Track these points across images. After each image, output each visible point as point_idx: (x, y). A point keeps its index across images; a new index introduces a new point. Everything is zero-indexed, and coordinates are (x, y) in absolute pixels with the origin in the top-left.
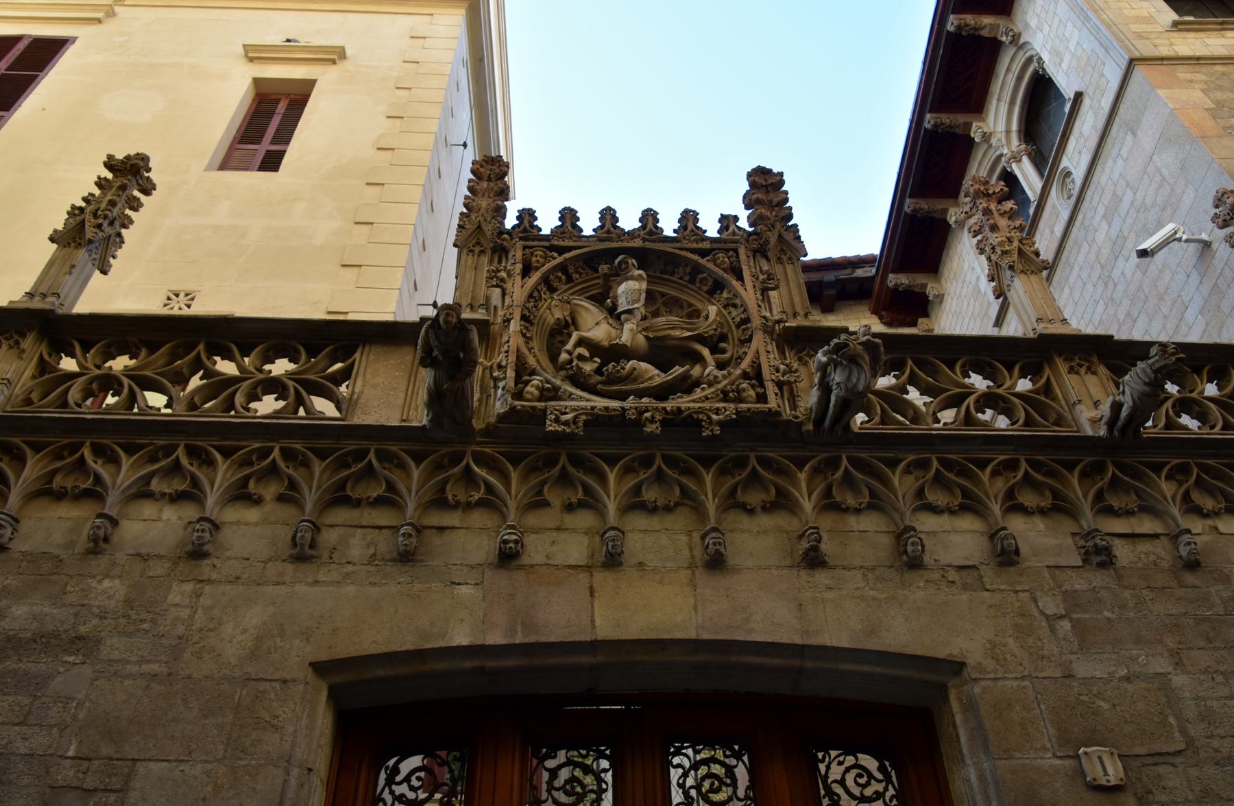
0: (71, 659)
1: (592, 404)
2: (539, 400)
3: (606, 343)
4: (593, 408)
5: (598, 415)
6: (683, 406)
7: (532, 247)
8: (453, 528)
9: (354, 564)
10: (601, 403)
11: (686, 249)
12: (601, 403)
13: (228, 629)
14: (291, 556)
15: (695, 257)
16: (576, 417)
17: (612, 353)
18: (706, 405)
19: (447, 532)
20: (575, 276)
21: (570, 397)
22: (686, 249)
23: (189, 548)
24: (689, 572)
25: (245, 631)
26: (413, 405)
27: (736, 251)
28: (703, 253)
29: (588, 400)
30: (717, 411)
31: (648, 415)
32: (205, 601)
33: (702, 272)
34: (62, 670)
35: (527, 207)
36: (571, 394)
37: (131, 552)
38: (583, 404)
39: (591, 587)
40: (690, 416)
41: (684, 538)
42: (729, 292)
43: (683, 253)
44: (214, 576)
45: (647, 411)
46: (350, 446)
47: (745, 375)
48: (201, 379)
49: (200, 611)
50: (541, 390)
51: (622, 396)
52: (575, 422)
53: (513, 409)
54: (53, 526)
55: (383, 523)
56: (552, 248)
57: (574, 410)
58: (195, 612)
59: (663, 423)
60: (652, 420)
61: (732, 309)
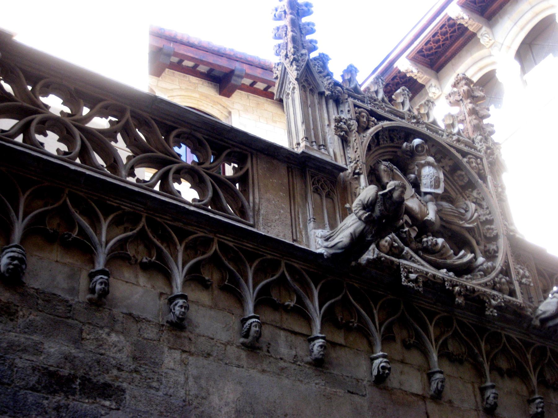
0: (107, 403)
1: (426, 269)
2: (387, 254)
3: (419, 216)
4: (427, 273)
5: (429, 280)
6: (477, 287)
7: (359, 107)
8: (341, 345)
9: (285, 361)
10: (431, 271)
11: (454, 148)
12: (431, 271)
13: (215, 400)
14: (243, 344)
15: (459, 156)
16: (417, 278)
17: (424, 227)
18: (488, 291)
19: (338, 348)
20: (381, 142)
21: (411, 259)
22: (454, 148)
23: (185, 323)
24: (476, 413)
25: (227, 404)
26: (298, 229)
27: (481, 159)
28: (464, 154)
29: (422, 265)
30: (494, 297)
31: (457, 288)
32: (193, 371)
33: (462, 170)
34: (103, 412)
35: (356, 66)
36: (412, 257)
37: (125, 311)
38: (421, 267)
39: (427, 413)
40: (478, 296)
41: (470, 386)
42: (479, 194)
43: (452, 150)
44: (193, 350)
45: (457, 285)
46: (127, 207)
47: (501, 272)
48: (116, 141)
49: (191, 379)
50: (391, 246)
51: (438, 267)
52: (416, 281)
53: (379, 258)
54: (51, 271)
55: (297, 329)
56: (372, 113)
57: (416, 272)
58: (187, 379)
59: (466, 297)
60: (459, 293)
61: (478, 208)
